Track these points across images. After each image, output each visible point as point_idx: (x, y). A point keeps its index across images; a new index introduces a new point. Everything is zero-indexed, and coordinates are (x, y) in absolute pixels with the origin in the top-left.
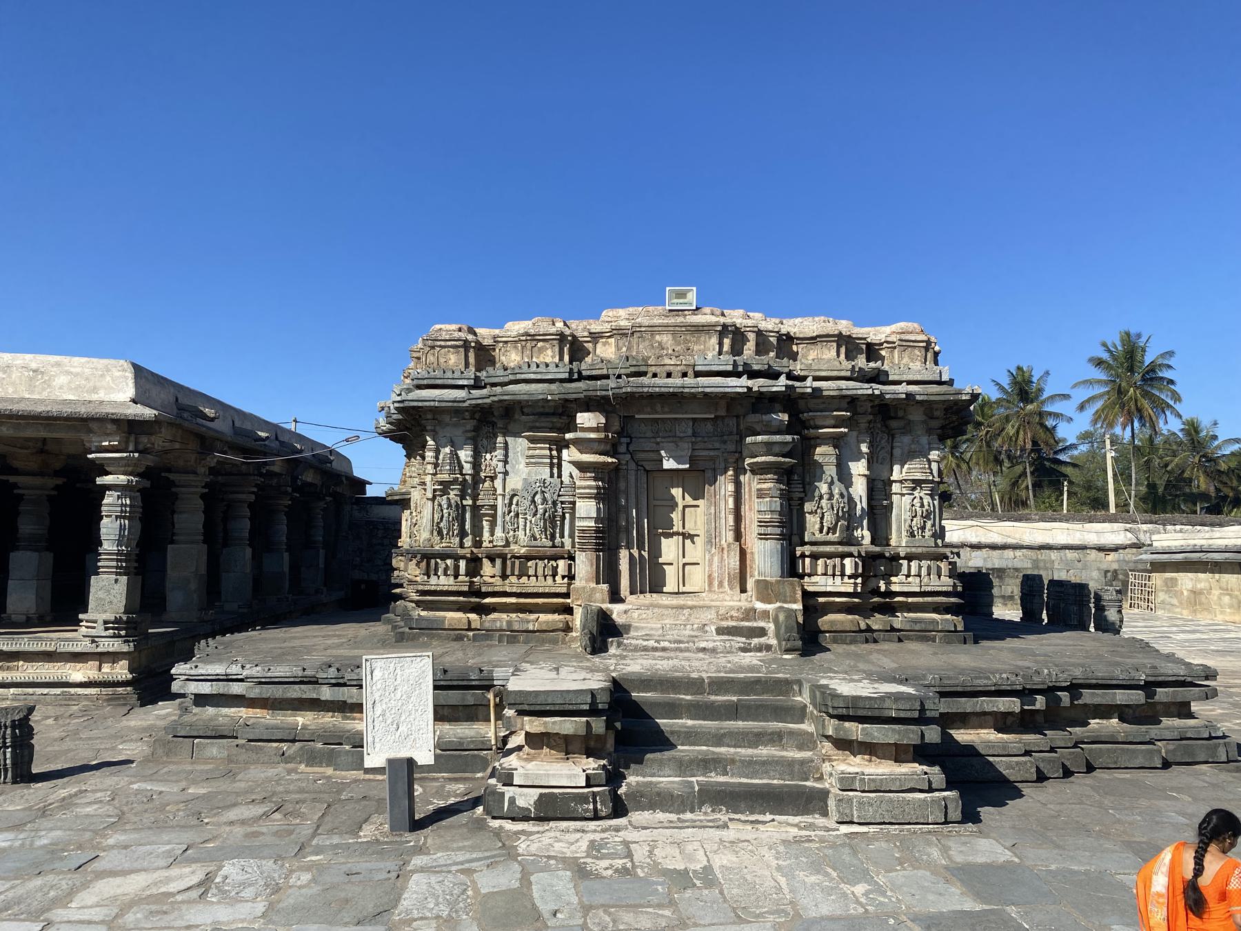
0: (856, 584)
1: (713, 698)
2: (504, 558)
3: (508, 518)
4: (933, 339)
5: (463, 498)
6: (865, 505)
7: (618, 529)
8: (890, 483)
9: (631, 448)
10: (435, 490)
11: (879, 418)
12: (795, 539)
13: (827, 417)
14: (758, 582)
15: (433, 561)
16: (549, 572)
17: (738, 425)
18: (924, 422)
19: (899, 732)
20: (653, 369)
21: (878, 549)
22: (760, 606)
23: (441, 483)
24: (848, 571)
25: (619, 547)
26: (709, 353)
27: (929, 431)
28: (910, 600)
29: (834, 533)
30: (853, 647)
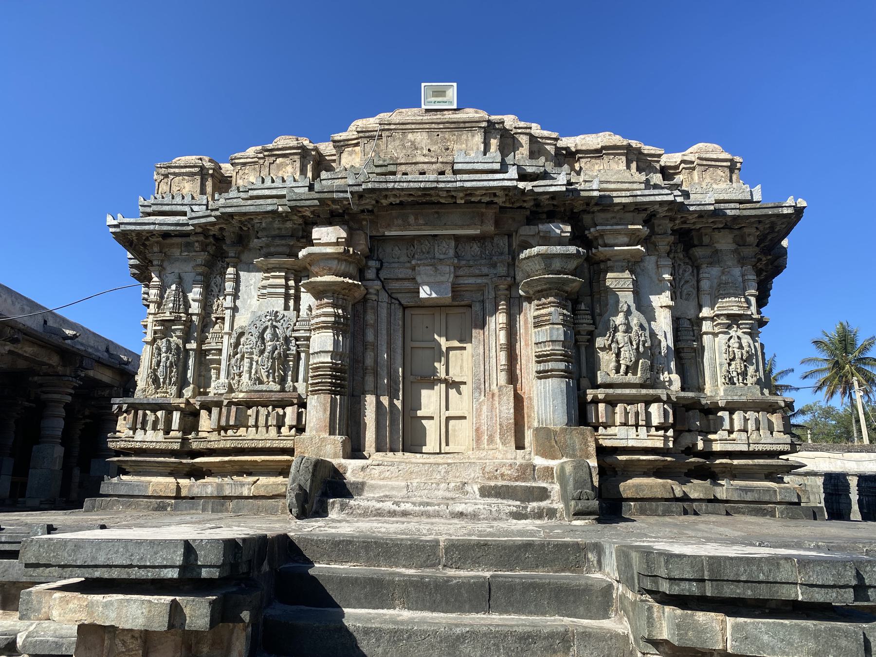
0: (666, 438)
1: (451, 572)
2: (219, 404)
3: (233, 361)
4: (738, 159)
5: (186, 340)
6: (671, 344)
7: (364, 370)
8: (699, 321)
9: (382, 275)
10: (155, 332)
11: (680, 247)
12: (584, 382)
13: (618, 232)
14: (537, 430)
15: (140, 413)
16: (272, 421)
17: (510, 245)
18: (735, 251)
19: (816, 635)
20: (403, 168)
21: (690, 394)
22: (540, 462)
23: (163, 322)
24: (656, 420)
25: (364, 393)
26: (471, 152)
27: (742, 261)
28: (736, 462)
29: (635, 373)
30: (667, 519)
